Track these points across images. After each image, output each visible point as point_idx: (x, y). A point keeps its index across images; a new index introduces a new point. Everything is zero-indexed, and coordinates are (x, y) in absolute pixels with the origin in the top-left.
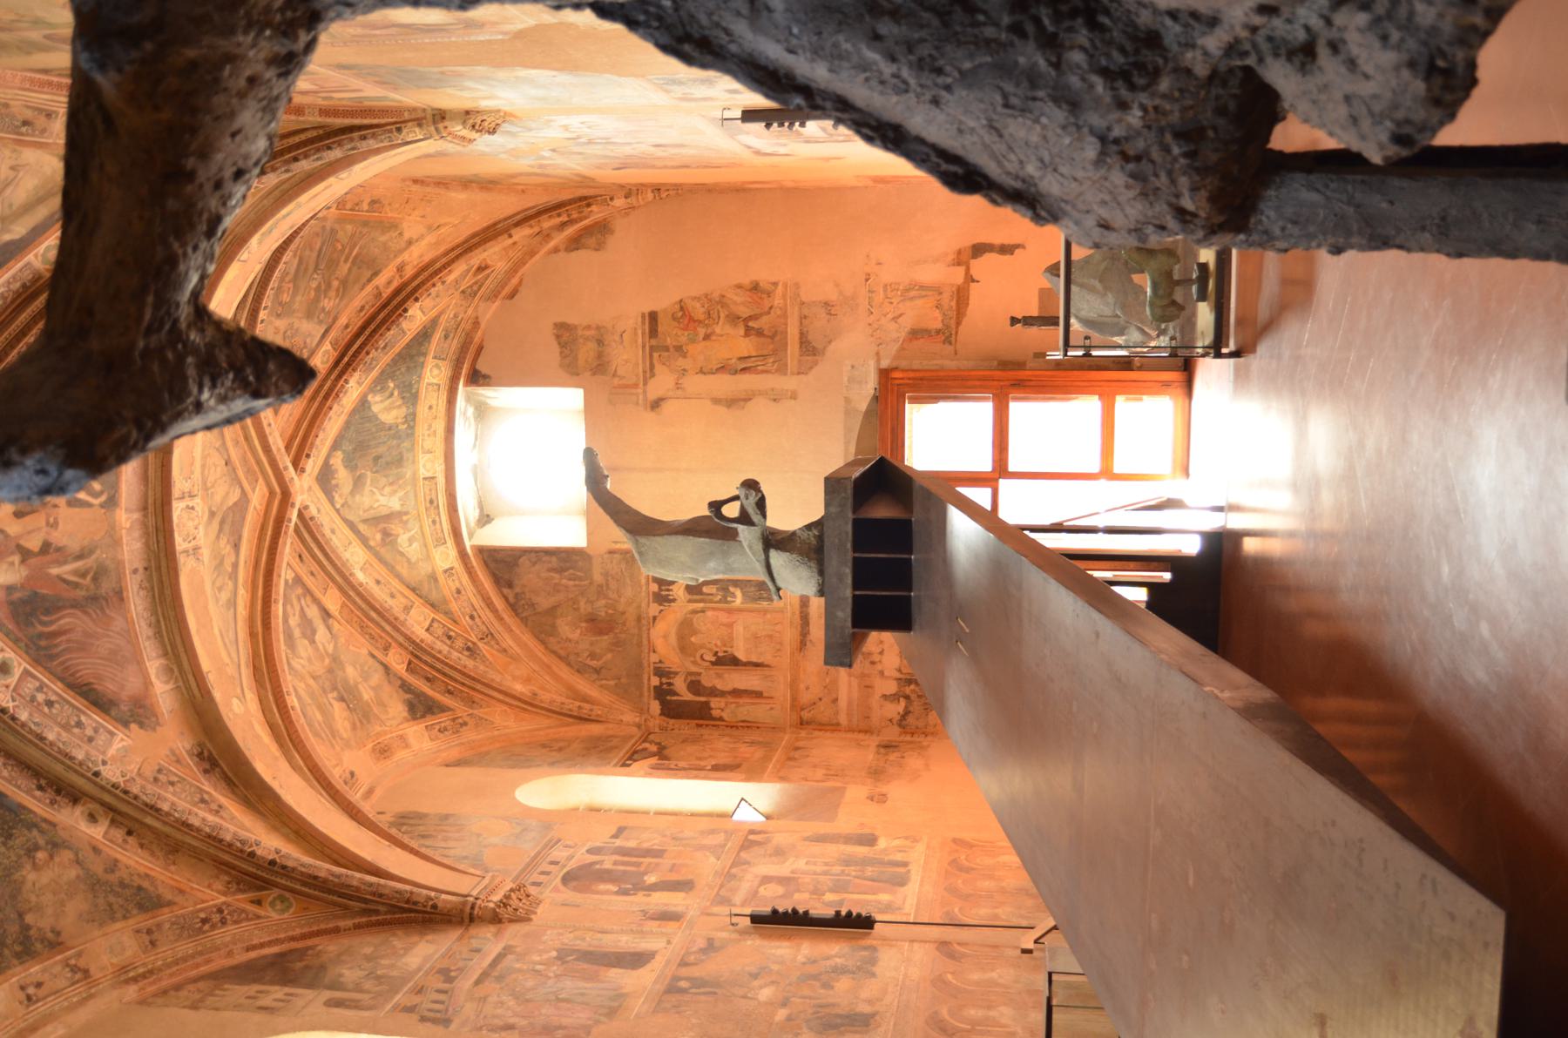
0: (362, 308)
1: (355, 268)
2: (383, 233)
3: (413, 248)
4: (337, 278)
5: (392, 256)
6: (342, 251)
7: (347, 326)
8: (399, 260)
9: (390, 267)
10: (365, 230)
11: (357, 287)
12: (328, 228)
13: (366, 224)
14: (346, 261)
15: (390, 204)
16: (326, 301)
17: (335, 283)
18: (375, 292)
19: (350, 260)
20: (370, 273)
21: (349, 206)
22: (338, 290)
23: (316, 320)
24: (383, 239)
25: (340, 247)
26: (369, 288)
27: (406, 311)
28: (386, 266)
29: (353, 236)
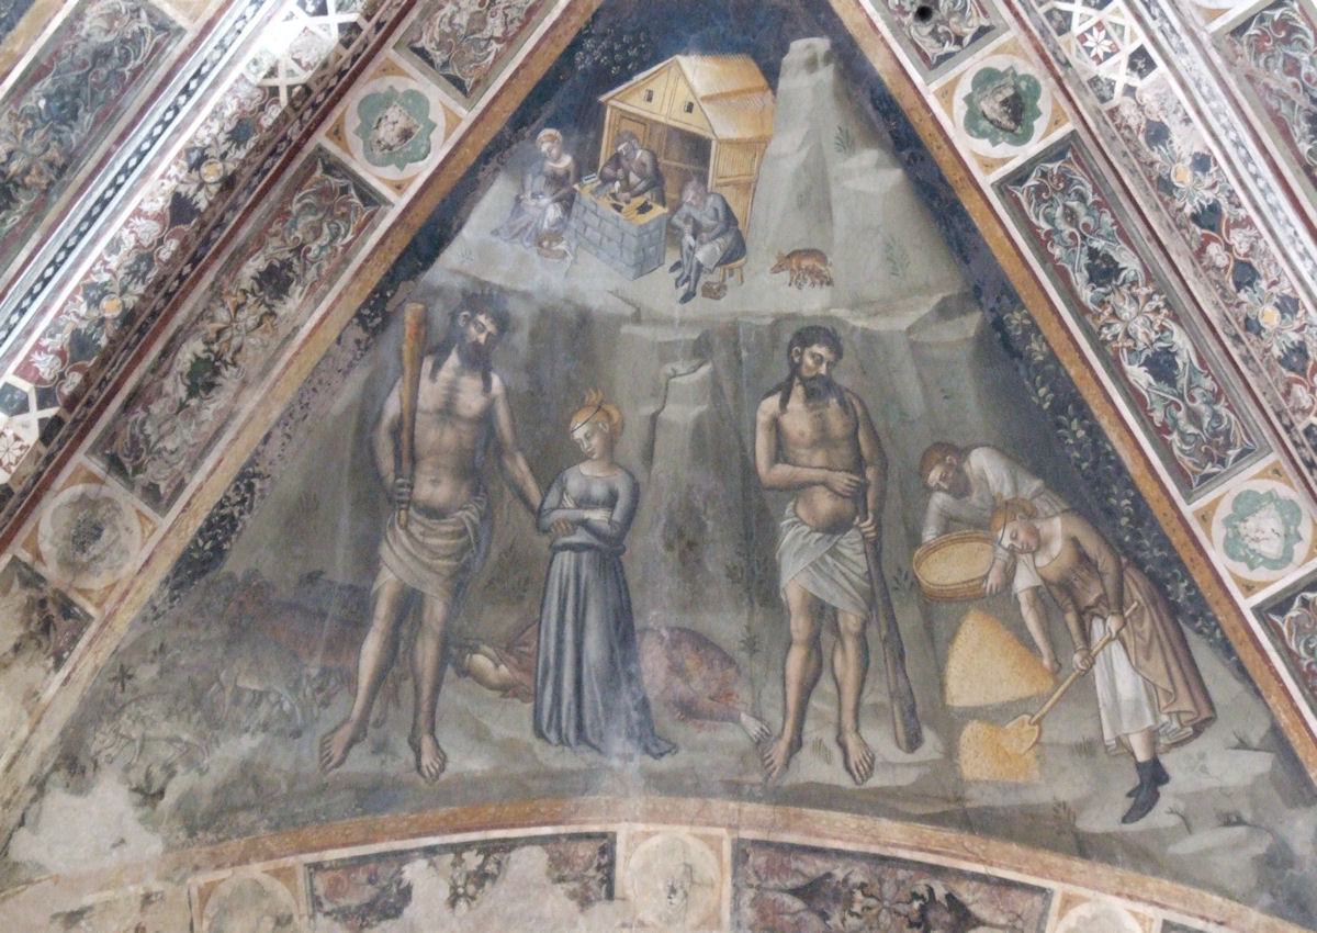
0: (204, 378)
1: (340, 568)
2: (249, 773)
3: (47, 739)
4: (434, 512)
5: (146, 674)
6: (453, 651)
7: (276, 281)
8: (89, 658)
9: (126, 616)
10: (361, 763)
11: (286, 479)
12: (619, 744)
13: (372, 796)
14: (409, 605)
15: (282, 921)
16: (471, 399)
17: (434, 487)
18: (156, 473)
19: (382, 610)
20: (237, 562)
21: (528, 863)
22: (408, 456)
23: (520, 311)
24: (240, 747)
25: (481, 661)
26: (209, 484)
27: (49, 430)
28: (153, 613)
29: (426, 722)
